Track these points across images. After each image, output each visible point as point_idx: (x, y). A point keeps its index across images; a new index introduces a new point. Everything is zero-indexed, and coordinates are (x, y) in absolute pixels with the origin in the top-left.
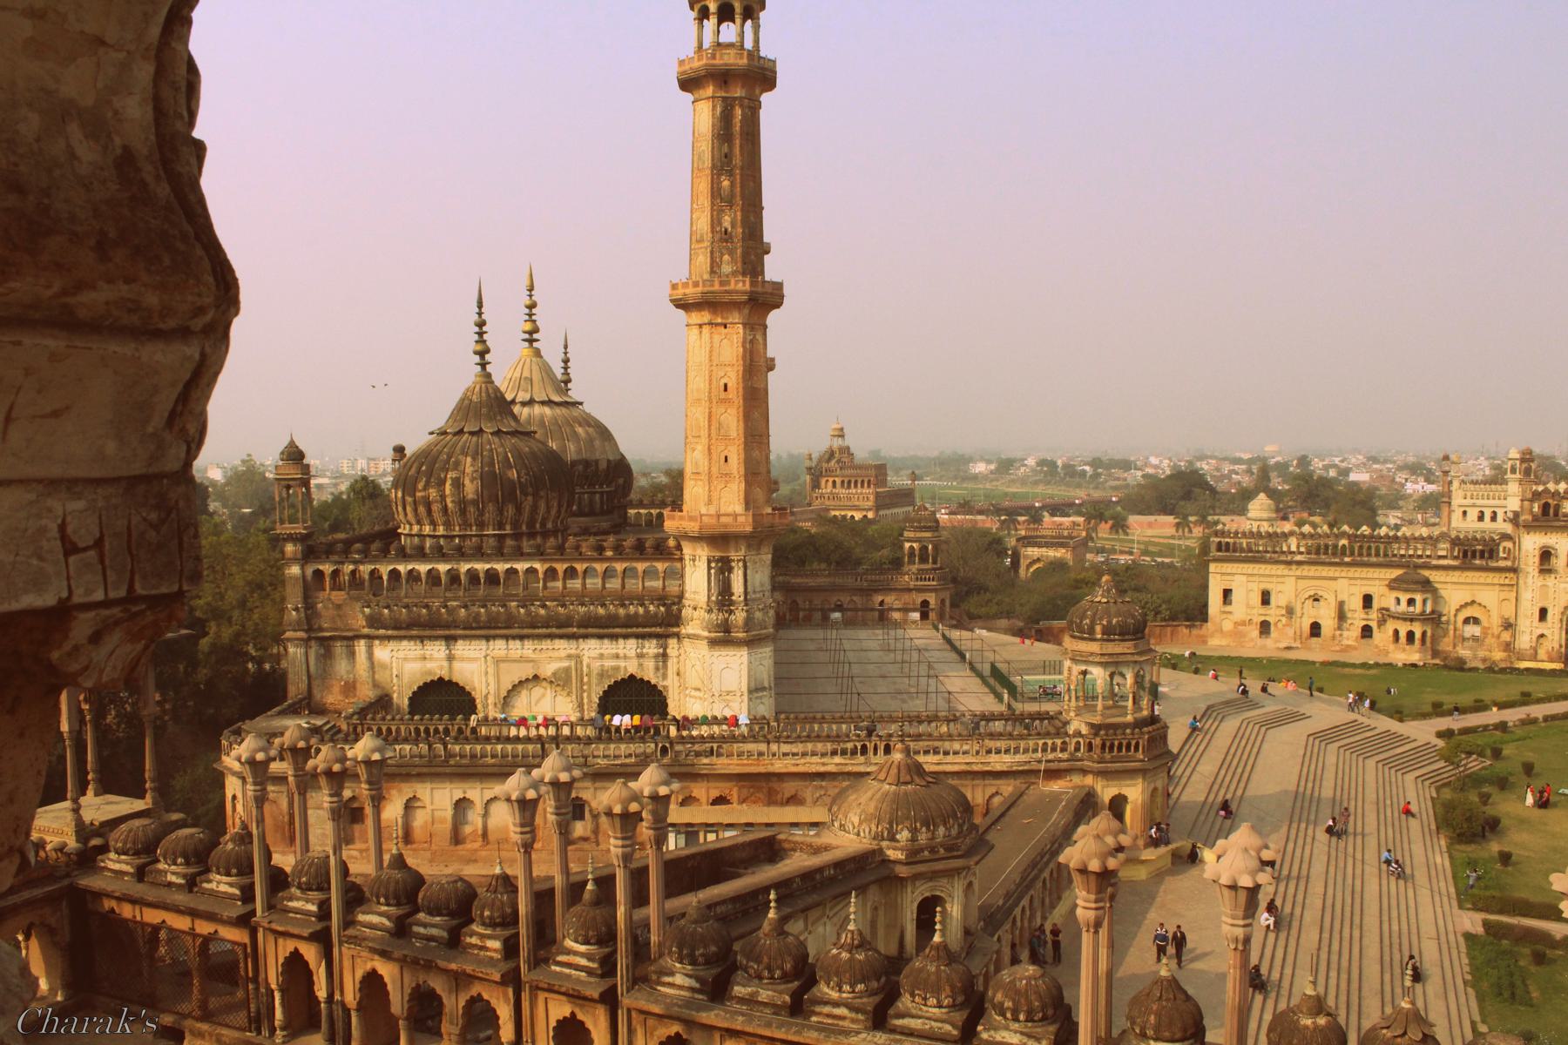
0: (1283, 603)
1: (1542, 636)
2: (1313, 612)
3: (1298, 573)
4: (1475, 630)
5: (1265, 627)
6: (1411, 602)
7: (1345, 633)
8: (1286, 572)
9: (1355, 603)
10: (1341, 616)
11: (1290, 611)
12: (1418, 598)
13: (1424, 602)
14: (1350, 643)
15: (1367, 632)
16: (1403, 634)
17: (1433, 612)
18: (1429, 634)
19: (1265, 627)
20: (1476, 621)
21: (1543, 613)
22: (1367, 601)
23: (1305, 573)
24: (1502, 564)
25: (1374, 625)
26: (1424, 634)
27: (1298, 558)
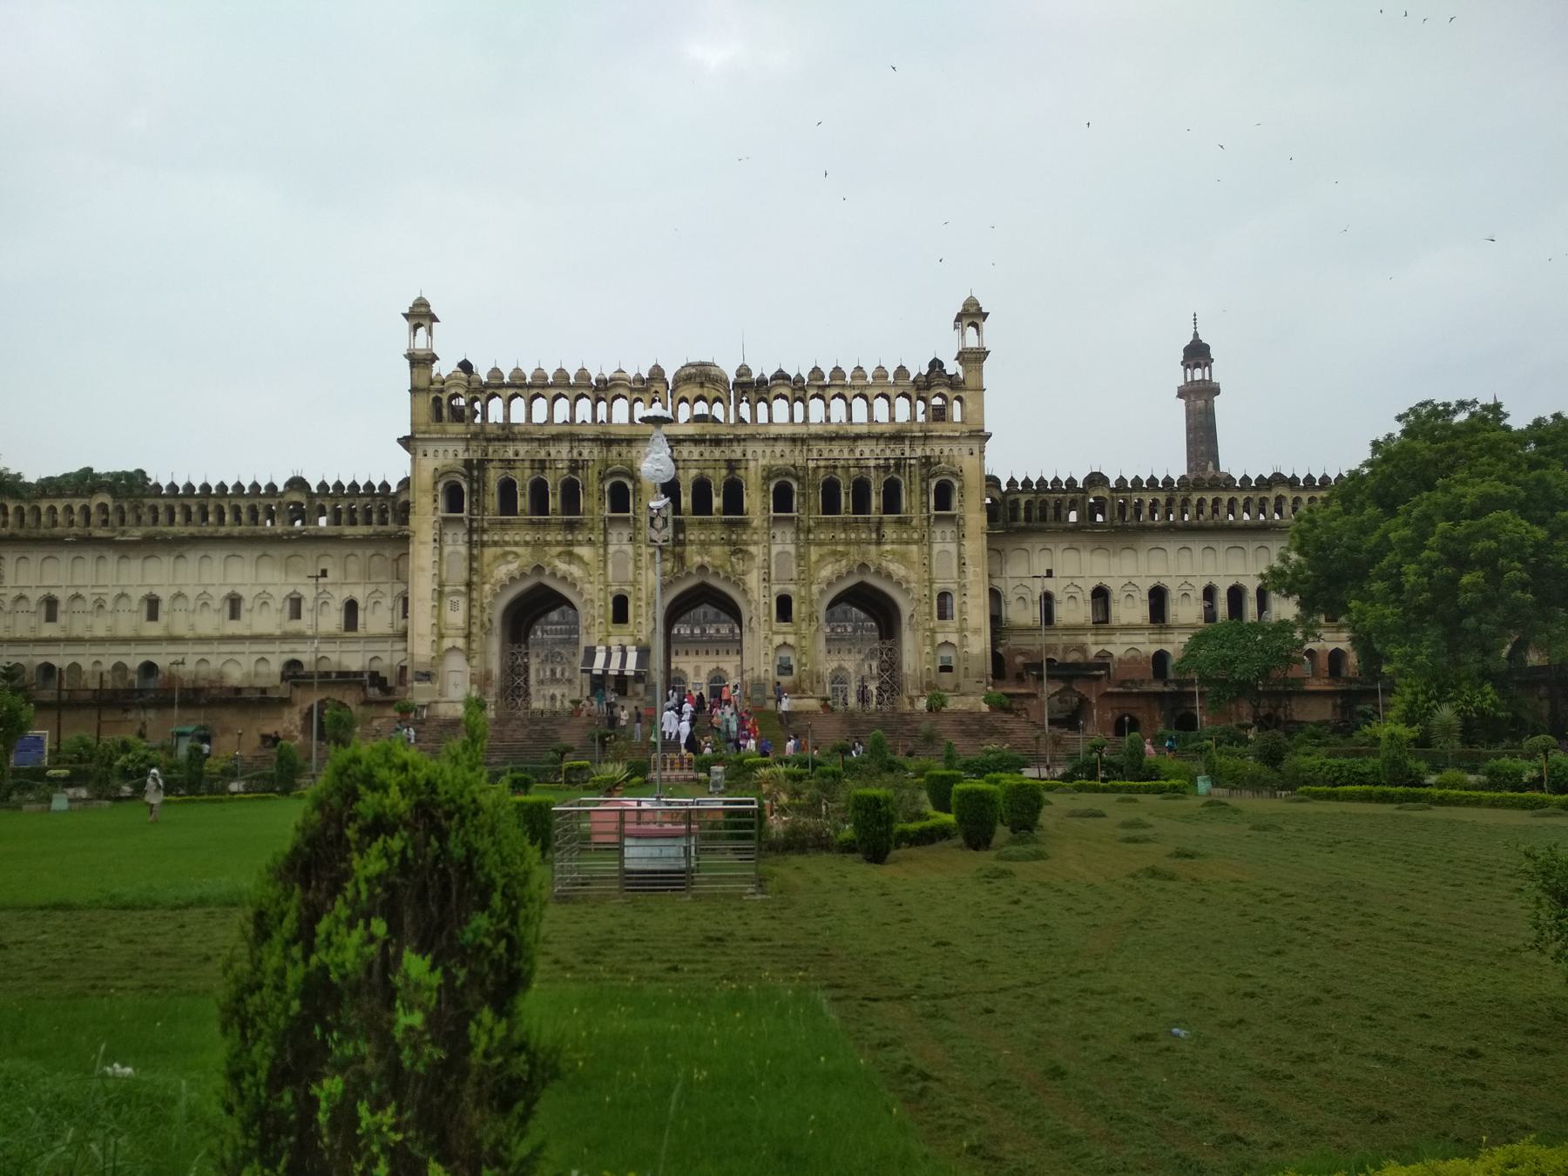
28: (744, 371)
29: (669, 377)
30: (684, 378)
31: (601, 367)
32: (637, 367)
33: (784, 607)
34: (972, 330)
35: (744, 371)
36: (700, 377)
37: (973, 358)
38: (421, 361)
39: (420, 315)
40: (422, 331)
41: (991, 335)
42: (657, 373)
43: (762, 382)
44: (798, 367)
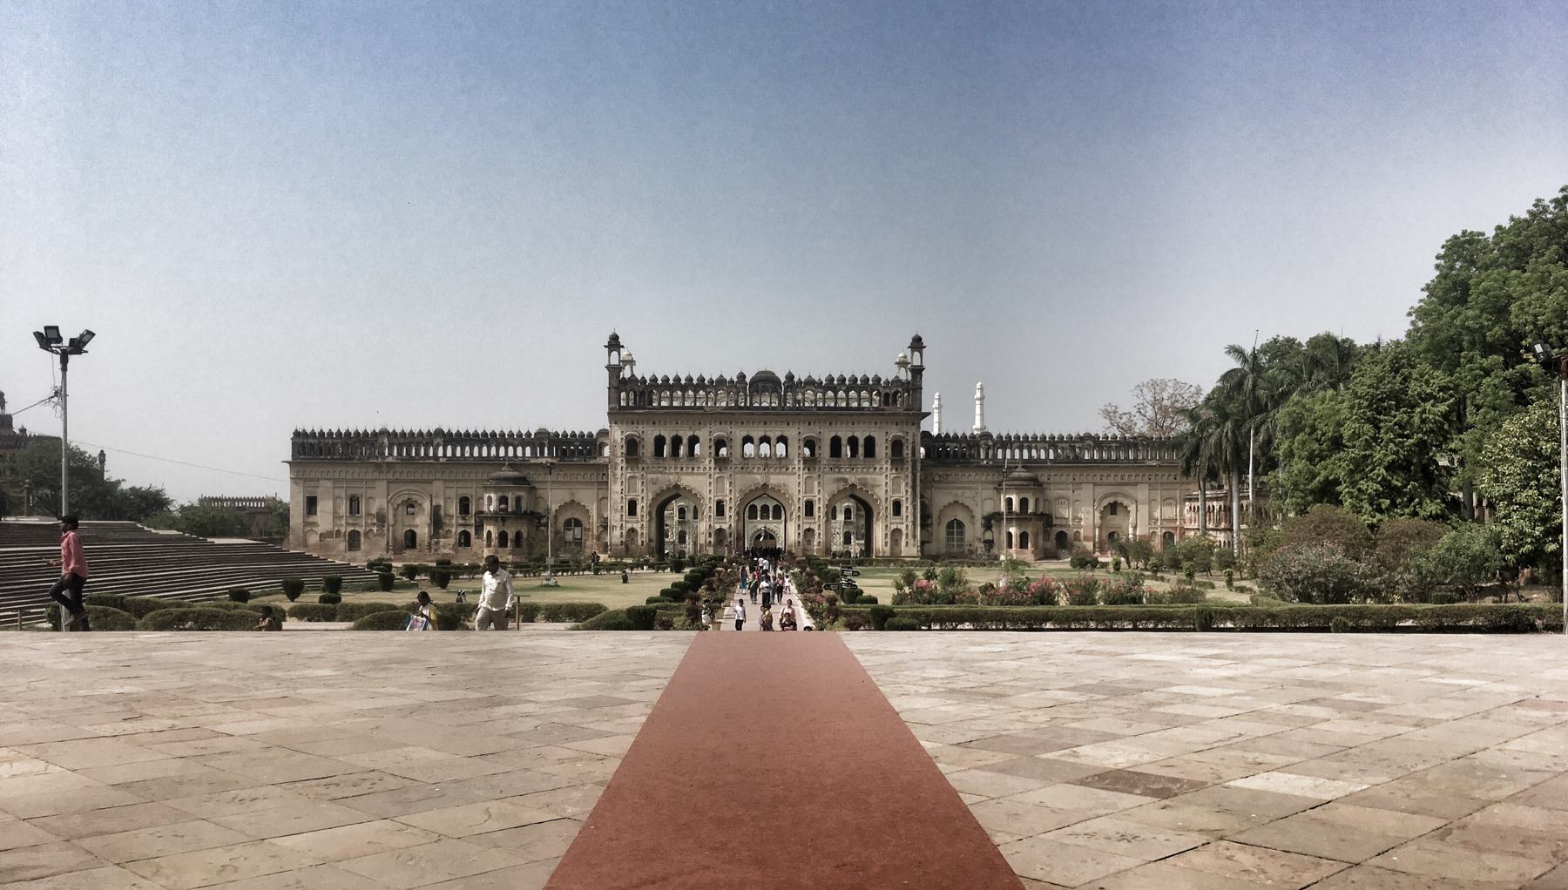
0: (374, 511)
1: (633, 530)
2: (407, 519)
3: (390, 476)
4: (577, 530)
5: (353, 541)
6: (503, 500)
7: (442, 541)
8: (376, 475)
9: (454, 509)
10: (437, 522)
11: (381, 519)
12: (510, 496)
13: (518, 500)
14: (447, 551)
15: (465, 540)
16: (494, 535)
17: (532, 513)
18: (525, 535)
19: (353, 541)
20: (578, 523)
21: (632, 507)
22: (464, 505)
23: (397, 476)
24: (599, 461)
25: (472, 531)
26: (518, 535)
27: (390, 459)
28: (790, 377)
29: (748, 380)
30: (754, 381)
31: (711, 374)
32: (731, 375)
33: (809, 507)
34: (917, 354)
35: (790, 377)
36: (766, 382)
37: (917, 371)
38: (614, 370)
39: (614, 344)
40: (615, 353)
41: (930, 359)
42: (742, 377)
43: (800, 382)
44: (820, 375)
